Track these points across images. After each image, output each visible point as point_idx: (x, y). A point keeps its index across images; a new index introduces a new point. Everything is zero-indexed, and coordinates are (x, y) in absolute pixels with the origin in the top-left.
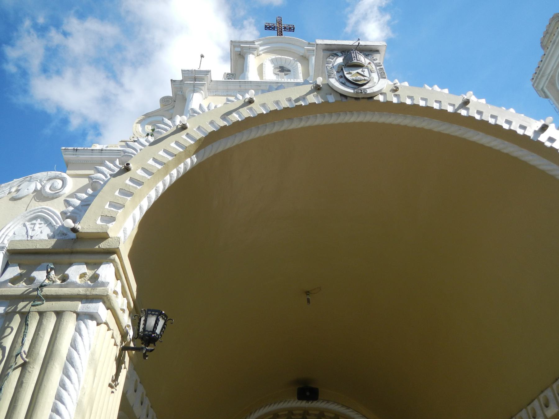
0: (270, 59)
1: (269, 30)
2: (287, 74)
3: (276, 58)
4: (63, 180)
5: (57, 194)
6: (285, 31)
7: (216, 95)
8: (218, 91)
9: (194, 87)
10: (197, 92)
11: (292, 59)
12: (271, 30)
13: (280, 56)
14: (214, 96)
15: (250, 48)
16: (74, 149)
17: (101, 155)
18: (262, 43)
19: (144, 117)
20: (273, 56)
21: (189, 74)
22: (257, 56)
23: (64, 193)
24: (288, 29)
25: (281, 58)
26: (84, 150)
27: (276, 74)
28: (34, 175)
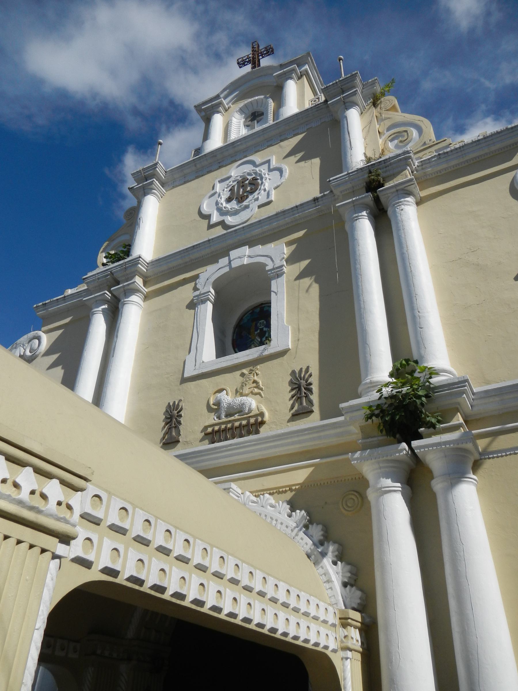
0: (238, 109)
1: (245, 65)
2: (261, 120)
3: (245, 105)
4: (39, 338)
5: (34, 355)
6: (263, 57)
7: (174, 187)
8: (176, 181)
9: (144, 190)
10: (148, 194)
11: (262, 97)
12: (247, 65)
13: (250, 100)
14: (171, 189)
15: (213, 107)
16: (43, 304)
17: (65, 303)
18: (228, 92)
19: (108, 242)
20: (241, 104)
21: (138, 175)
22: (226, 111)
23: (40, 353)
24: (266, 53)
25: (251, 102)
26: (51, 302)
27: (248, 126)
28: (18, 341)
